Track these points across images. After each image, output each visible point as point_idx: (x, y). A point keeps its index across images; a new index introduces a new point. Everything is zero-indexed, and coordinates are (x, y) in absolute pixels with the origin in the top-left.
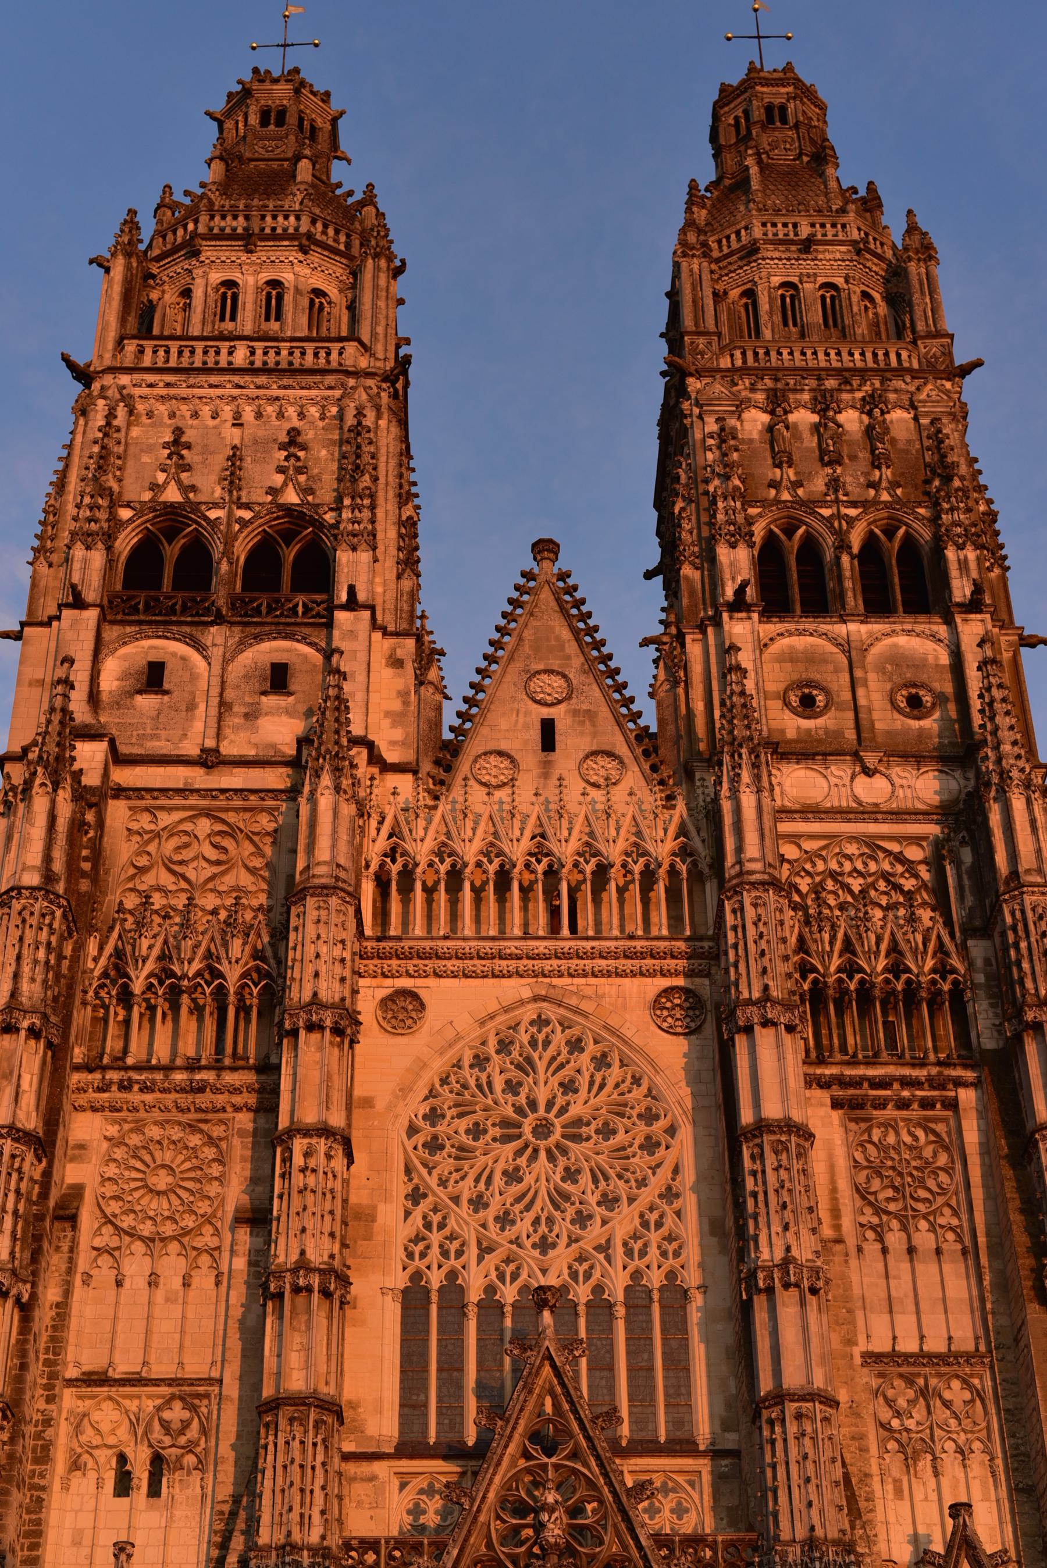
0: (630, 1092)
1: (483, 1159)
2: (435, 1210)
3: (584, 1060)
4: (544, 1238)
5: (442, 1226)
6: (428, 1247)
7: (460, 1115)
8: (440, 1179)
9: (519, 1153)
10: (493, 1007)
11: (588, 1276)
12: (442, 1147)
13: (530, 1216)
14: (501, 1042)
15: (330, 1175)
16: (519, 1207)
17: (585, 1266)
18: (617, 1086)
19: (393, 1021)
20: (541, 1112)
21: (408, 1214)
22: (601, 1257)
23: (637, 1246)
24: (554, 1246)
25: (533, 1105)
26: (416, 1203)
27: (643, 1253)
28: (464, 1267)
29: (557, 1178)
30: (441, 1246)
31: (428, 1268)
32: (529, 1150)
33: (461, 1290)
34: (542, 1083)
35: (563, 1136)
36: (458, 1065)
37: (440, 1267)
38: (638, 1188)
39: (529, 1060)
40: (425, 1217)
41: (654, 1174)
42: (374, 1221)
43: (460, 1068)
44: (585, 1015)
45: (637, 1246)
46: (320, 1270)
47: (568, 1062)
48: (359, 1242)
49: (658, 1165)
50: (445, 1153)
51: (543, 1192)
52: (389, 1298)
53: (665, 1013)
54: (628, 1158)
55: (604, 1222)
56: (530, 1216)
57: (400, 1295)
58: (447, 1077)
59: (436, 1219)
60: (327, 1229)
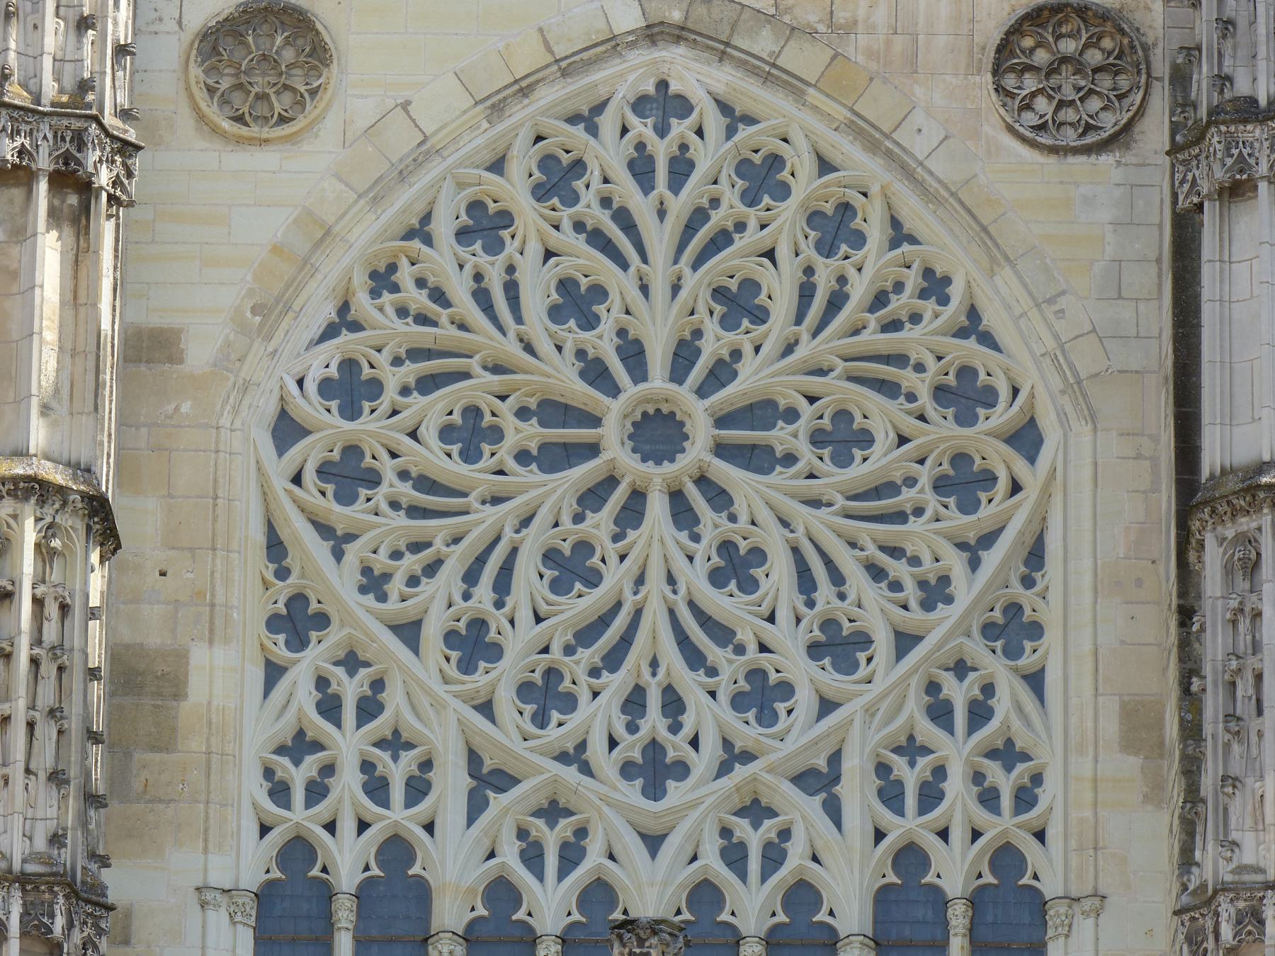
0: (916, 318)
1: (492, 514)
2: (352, 662)
3: (788, 214)
4: (654, 748)
5: (369, 709)
6: (328, 769)
7: (428, 384)
8: (366, 571)
9: (593, 497)
10: (528, 58)
11: (774, 856)
12: (373, 480)
13: (616, 684)
14: (547, 162)
15: (52, 610)
16: (588, 656)
17: (769, 828)
18: (879, 300)
19: (237, 97)
20: (658, 381)
21: (274, 673)
22: (813, 805)
23: (911, 776)
24: (681, 770)
25: (634, 354)
26: (299, 642)
27: (930, 796)
28: (429, 828)
29: (695, 578)
30: (367, 766)
31: (331, 827)
32: (618, 497)
33: (422, 893)
34: (660, 288)
35: (722, 450)
36: (421, 232)
37: (363, 826)
38: (927, 605)
39: (624, 219)
40: (322, 682)
41: (974, 564)
42: (179, 693)
43: (428, 240)
44: (793, 85)
45: (911, 776)
46: (23, 880)
47: (741, 226)
48: (138, 756)
49: (988, 540)
50: (381, 495)
51: (655, 618)
52: (218, 918)
53: (1031, 83)
54: (899, 517)
55: (827, 706)
56: (616, 684)
57: (251, 907)
58: (392, 268)
59: (350, 689)
60: (45, 759)
